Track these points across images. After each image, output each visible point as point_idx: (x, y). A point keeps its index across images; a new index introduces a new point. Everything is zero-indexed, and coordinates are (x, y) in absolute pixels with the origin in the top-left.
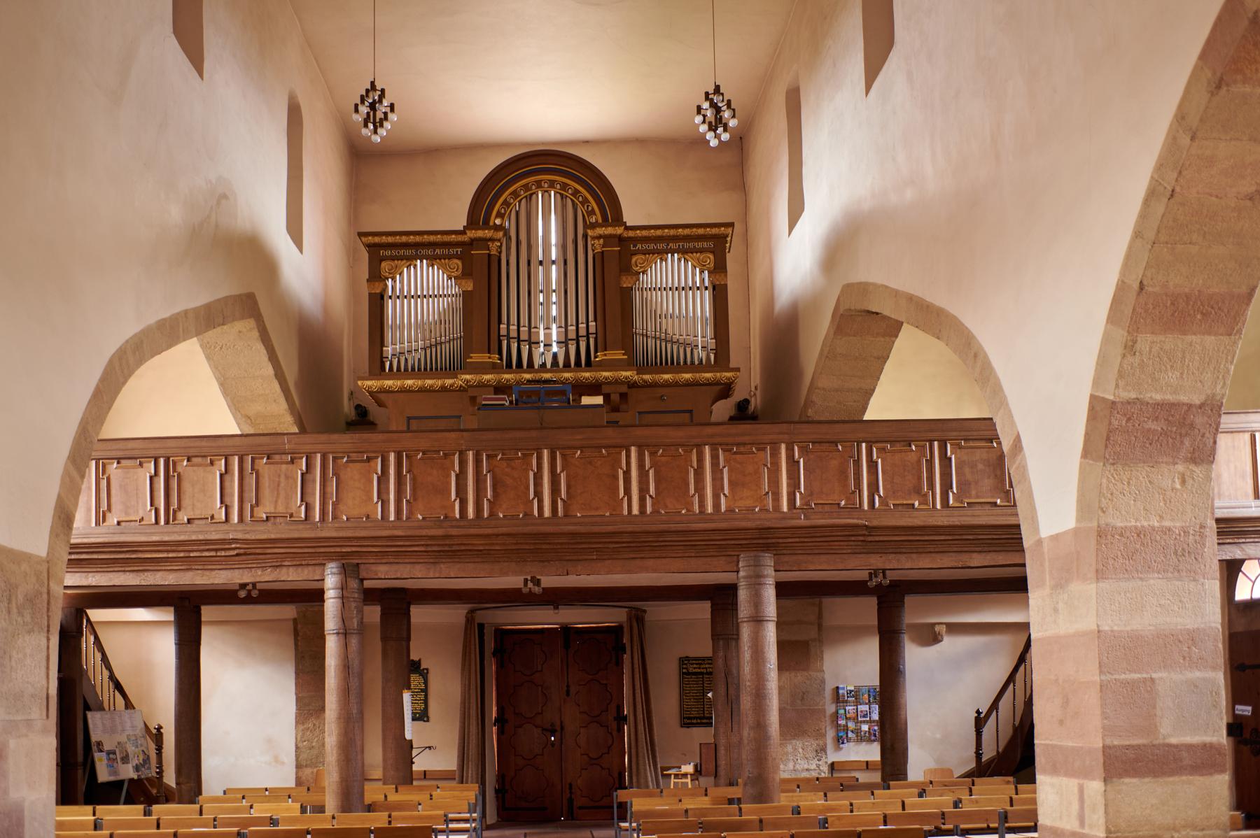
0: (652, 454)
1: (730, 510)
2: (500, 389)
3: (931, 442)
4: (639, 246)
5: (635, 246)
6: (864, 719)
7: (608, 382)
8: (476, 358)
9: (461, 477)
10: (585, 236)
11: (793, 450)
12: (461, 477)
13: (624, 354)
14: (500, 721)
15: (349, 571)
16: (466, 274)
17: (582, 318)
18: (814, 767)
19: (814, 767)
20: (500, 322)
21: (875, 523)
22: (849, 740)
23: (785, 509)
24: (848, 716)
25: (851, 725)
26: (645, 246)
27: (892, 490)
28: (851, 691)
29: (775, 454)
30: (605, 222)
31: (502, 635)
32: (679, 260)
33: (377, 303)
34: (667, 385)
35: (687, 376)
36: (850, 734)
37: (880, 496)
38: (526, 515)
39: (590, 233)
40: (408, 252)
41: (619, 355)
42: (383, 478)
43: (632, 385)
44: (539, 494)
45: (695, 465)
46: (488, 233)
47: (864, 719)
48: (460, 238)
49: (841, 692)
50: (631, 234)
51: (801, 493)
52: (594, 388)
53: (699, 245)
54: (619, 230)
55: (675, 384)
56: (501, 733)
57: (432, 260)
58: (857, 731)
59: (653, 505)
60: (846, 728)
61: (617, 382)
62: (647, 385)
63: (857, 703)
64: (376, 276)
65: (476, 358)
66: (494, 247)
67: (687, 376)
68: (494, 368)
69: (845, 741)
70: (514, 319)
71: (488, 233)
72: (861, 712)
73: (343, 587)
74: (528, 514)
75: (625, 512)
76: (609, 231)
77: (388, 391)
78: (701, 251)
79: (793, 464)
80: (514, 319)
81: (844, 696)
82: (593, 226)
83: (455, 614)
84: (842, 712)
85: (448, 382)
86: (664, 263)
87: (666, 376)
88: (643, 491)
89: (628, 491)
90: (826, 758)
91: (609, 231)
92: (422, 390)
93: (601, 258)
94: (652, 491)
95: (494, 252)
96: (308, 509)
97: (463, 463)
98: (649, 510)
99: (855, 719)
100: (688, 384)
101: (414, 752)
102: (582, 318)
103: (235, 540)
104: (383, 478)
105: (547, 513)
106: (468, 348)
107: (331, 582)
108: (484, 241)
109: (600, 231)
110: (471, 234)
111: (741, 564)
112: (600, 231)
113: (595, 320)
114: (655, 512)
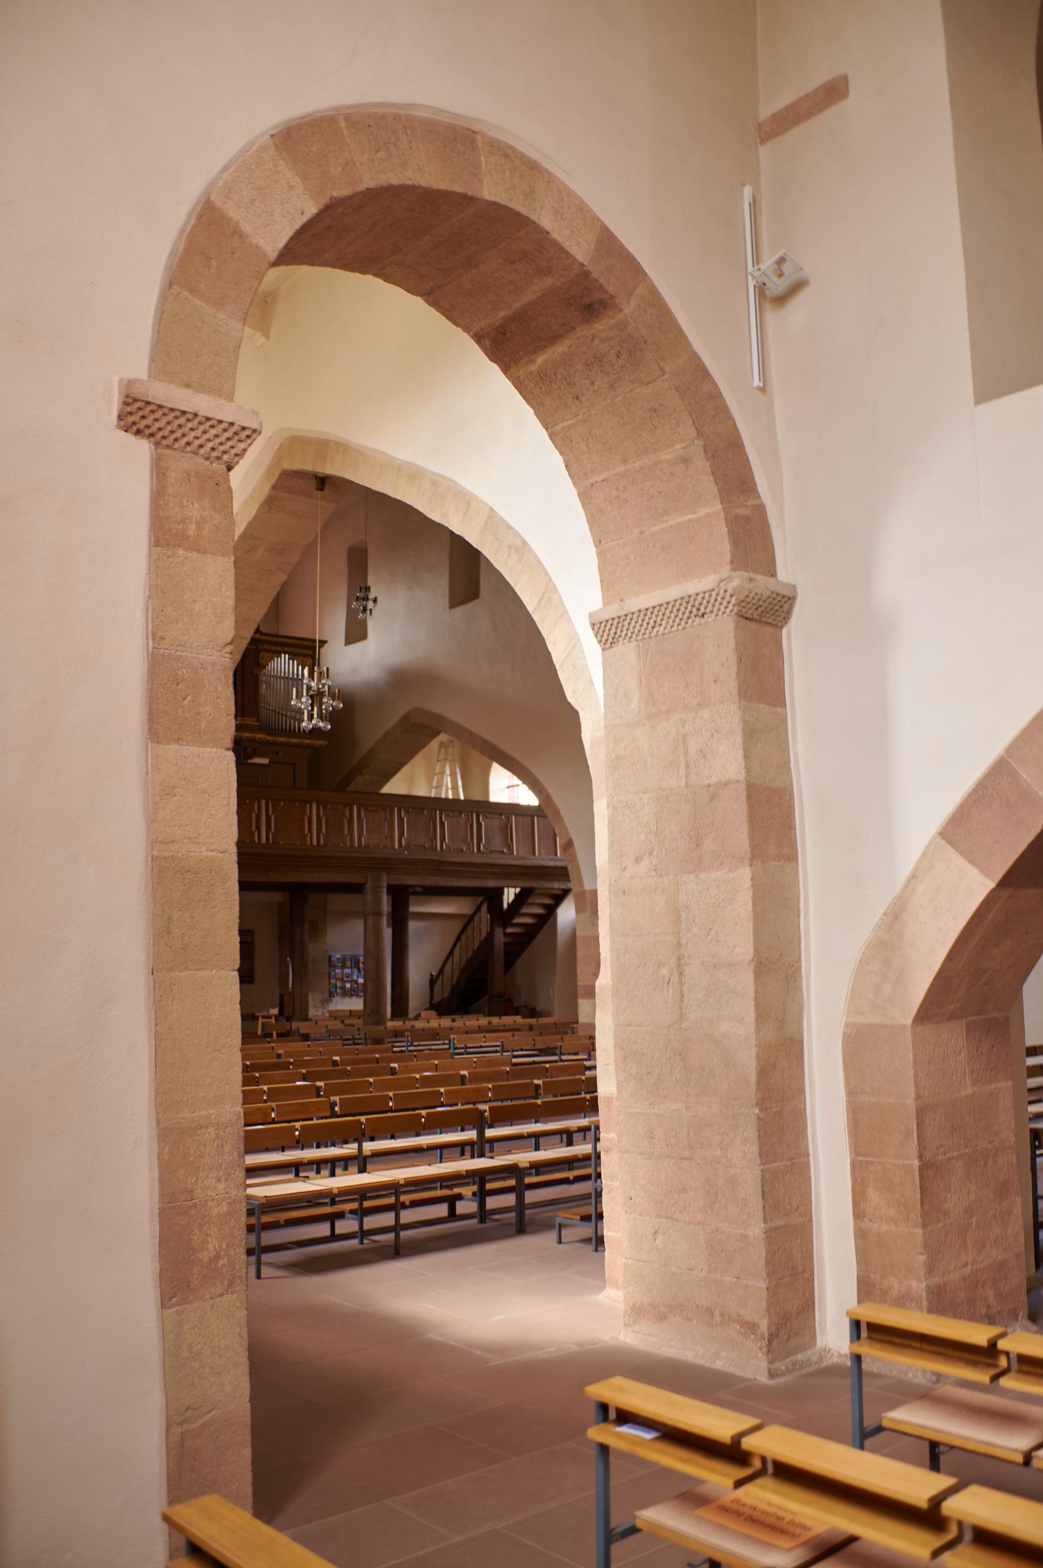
0: (324, 808)
1: (367, 846)
3: (472, 813)
4: (265, 646)
5: (262, 646)
6: (348, 979)
11: (401, 812)
13: (256, 721)
18: (320, 1013)
19: (320, 1013)
21: (445, 859)
22: (337, 995)
23: (397, 847)
24: (337, 976)
25: (339, 984)
26: (270, 647)
27: (451, 839)
28: (339, 959)
29: (392, 813)
32: (289, 659)
34: (281, 744)
35: (295, 740)
36: (338, 990)
37: (446, 843)
38: (250, 841)
44: (258, 828)
45: (348, 816)
47: (348, 979)
49: (333, 959)
50: (262, 638)
51: (405, 838)
53: (304, 651)
55: (288, 745)
58: (343, 988)
59: (324, 840)
60: (336, 986)
61: (254, 740)
62: (269, 743)
63: (344, 967)
67: (295, 740)
69: (335, 995)
72: (346, 974)
74: (252, 841)
75: (309, 843)
78: (305, 656)
79: (401, 819)
81: (334, 961)
84: (333, 973)
86: (279, 659)
87: (281, 739)
88: (319, 830)
90: (328, 1007)
98: (322, 842)
99: (342, 980)
100: (295, 745)
105: (264, 840)
111: (369, 879)
114: (325, 844)
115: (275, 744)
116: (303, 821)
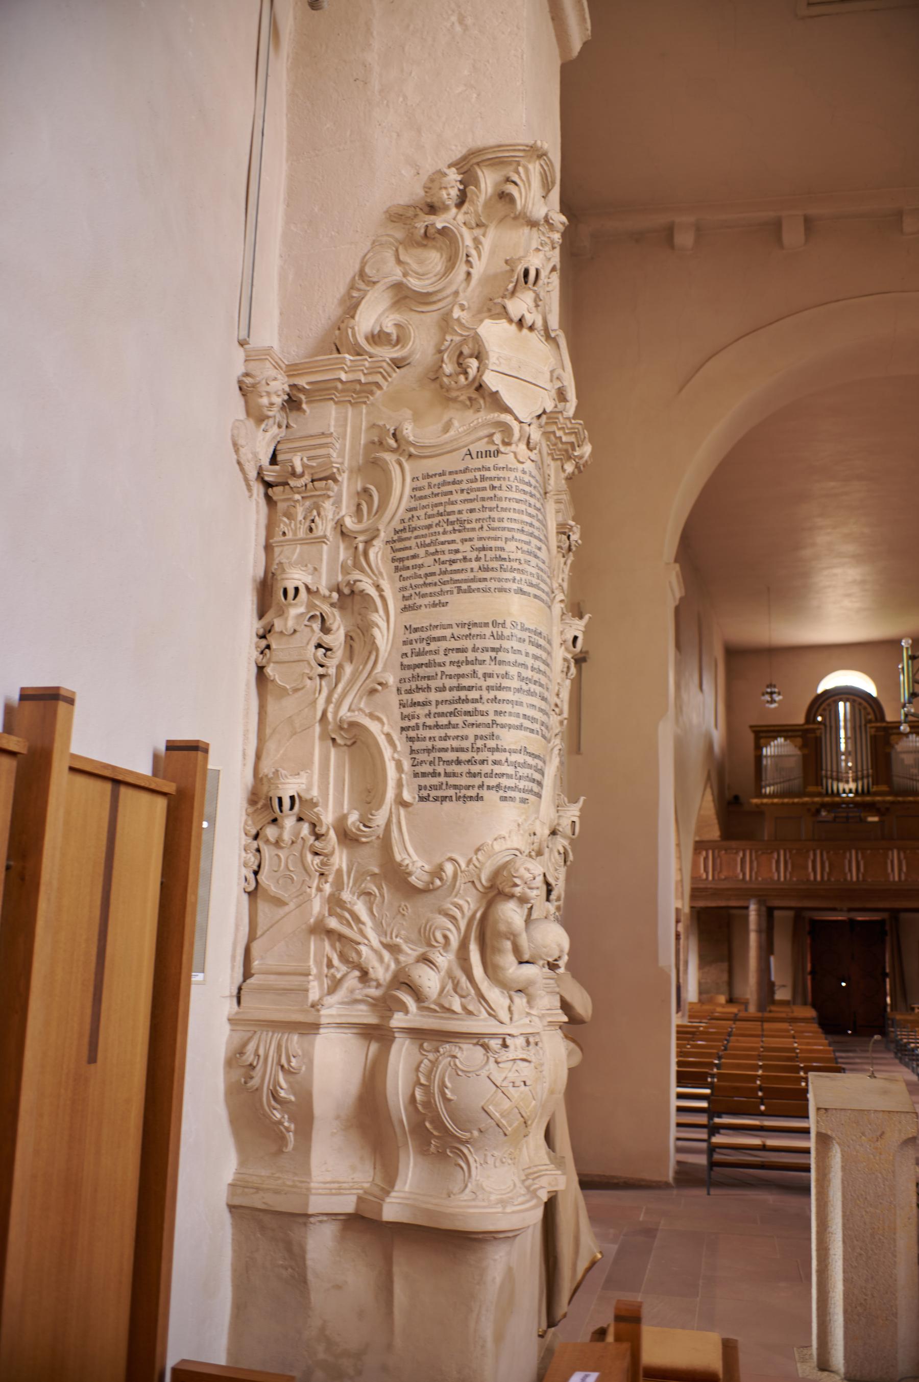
2: (824, 805)
7: (879, 802)
8: (811, 789)
9: (814, 862)
10: (865, 725)
12: (814, 862)
14: (812, 973)
15: (760, 903)
16: (803, 747)
17: (865, 767)
20: (822, 769)
30: (876, 720)
31: (814, 923)
33: (759, 758)
34: (910, 802)
39: (869, 725)
40: (775, 734)
41: (884, 788)
42: (778, 862)
43: (893, 803)
44: (850, 870)
46: (815, 726)
48: (801, 728)
50: (890, 725)
52: (871, 808)
54: (884, 725)
56: (813, 979)
57: (786, 738)
61: (884, 802)
62: (899, 802)
64: (758, 748)
65: (811, 789)
66: (818, 732)
68: (820, 795)
70: (829, 768)
71: (815, 726)
73: (759, 912)
74: (845, 880)
76: (878, 724)
77: (766, 804)
80: (829, 768)
82: (870, 721)
83: (791, 914)
85: (796, 800)
88: (900, 870)
89: (893, 870)
91: (878, 724)
92: (783, 804)
93: (874, 739)
94: (904, 869)
95: (818, 735)
96: (744, 875)
97: (815, 855)
101: (776, 988)
102: (865, 767)
103: (711, 888)
104: (778, 862)
106: (806, 783)
107: (753, 907)
108: (813, 730)
109: (873, 725)
110: (806, 727)
112: (873, 725)
113: (872, 768)
115: (904, 802)
116: (886, 863)
